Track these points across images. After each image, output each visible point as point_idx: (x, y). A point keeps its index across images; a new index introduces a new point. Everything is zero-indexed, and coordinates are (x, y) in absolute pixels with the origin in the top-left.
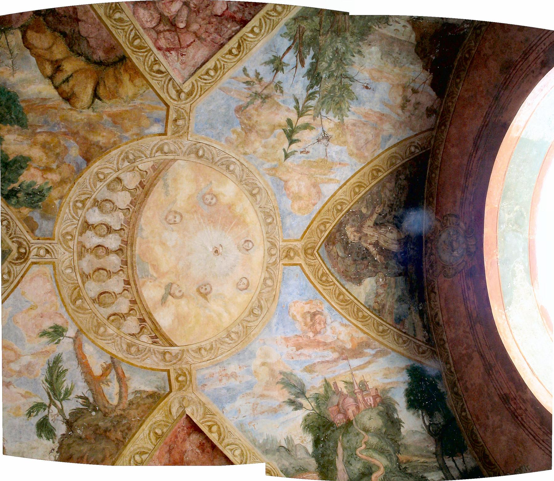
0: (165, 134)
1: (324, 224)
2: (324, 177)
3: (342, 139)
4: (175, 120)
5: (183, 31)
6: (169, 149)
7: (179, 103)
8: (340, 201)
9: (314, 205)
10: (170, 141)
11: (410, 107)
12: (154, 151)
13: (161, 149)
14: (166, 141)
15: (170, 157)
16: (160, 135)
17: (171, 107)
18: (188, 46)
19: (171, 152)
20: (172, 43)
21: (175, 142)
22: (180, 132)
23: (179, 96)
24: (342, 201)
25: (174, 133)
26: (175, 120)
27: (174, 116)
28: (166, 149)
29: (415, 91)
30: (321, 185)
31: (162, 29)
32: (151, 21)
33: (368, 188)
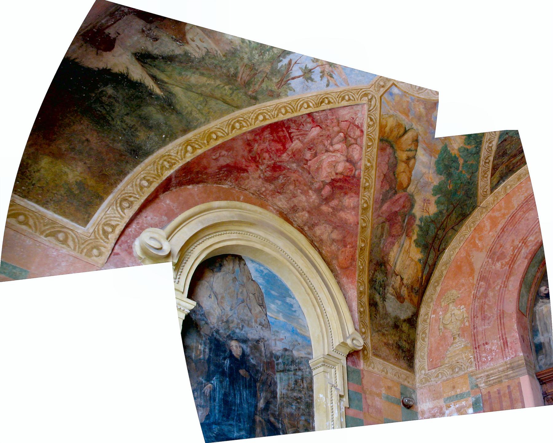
5: (343, 131)
18: (346, 121)
20: (353, 128)
31: (353, 140)
32: (355, 148)
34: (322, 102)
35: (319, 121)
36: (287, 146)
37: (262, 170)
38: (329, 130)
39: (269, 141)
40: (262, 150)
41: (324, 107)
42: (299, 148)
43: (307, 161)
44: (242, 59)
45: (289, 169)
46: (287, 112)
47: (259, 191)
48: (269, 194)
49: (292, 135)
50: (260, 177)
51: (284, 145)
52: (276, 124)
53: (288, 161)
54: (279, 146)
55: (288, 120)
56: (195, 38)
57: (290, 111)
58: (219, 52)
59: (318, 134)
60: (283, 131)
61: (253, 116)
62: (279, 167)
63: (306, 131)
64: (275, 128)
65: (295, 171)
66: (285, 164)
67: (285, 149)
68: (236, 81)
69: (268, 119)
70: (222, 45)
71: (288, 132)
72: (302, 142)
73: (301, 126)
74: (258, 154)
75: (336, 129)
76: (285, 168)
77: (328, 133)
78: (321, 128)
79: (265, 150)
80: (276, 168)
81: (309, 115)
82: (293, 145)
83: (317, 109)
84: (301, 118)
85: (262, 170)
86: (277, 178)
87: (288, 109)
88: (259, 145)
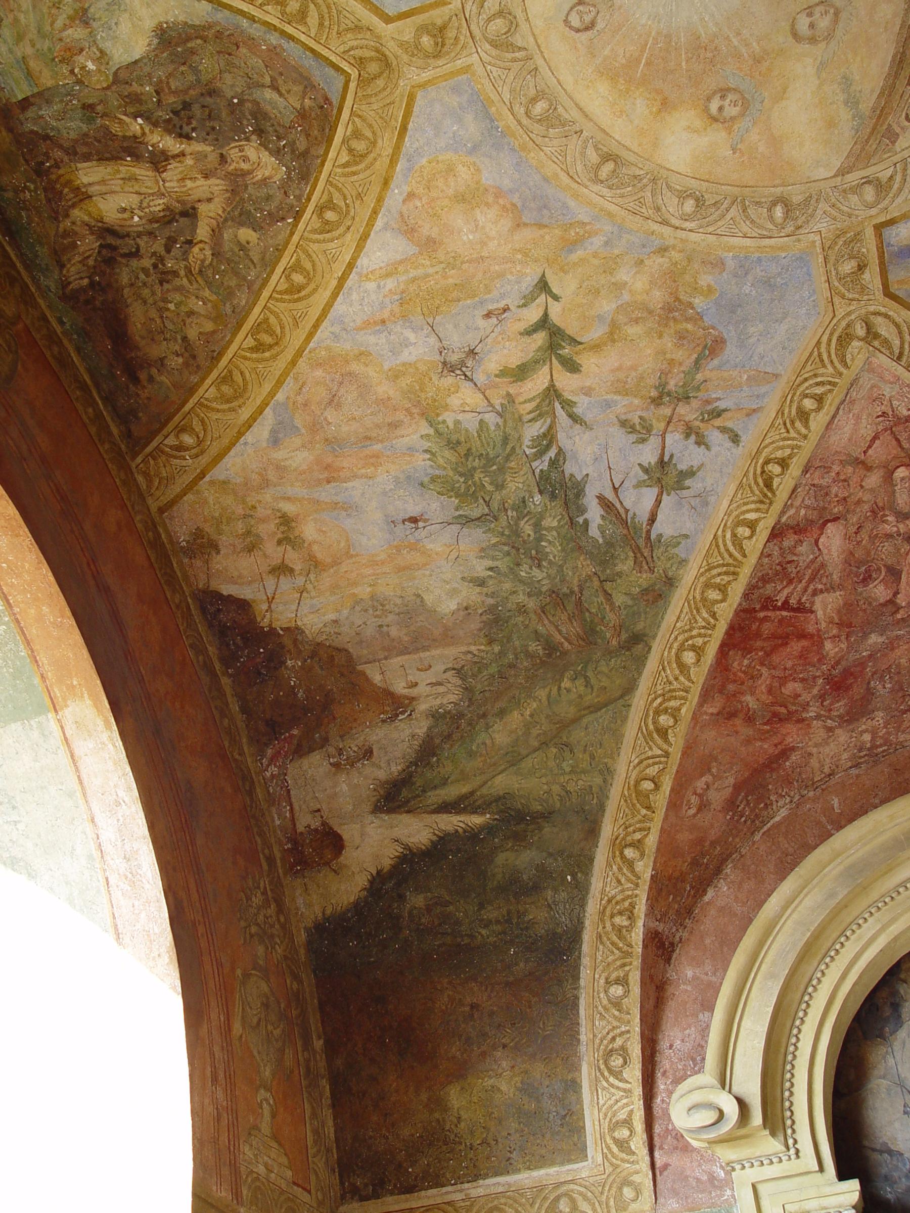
0: (879, 229)
1: (357, 157)
2: (413, 273)
3: (404, 382)
4: (861, 268)
6: (861, 195)
7: (863, 311)
8: (335, 234)
9: (411, 196)
10: (862, 214)
11: (267, 529)
12: (898, 178)
13: (882, 187)
14: (874, 211)
15: (853, 178)
16: (891, 222)
17: (879, 294)
19: (856, 189)
21: (850, 216)
22: (845, 242)
23: (869, 327)
24: (327, 236)
25: (858, 237)
26: (861, 268)
27: (867, 276)
28: (869, 193)
29: (282, 569)
30: (412, 250)
33: (266, 294)
34: (768, 485)
35: (814, 515)
36: (811, 629)
37: (818, 717)
38: (859, 502)
39: (762, 664)
40: (770, 691)
41: (783, 485)
42: (841, 602)
43: (891, 602)
44: (522, 609)
45: (870, 656)
46: (723, 589)
47: (860, 750)
48: (888, 733)
49: (793, 601)
50: (830, 730)
51: (802, 636)
52: (732, 629)
53: (850, 647)
54: (796, 646)
55: (746, 596)
56: (410, 678)
57: (726, 578)
58: (473, 648)
59: (847, 538)
60: (766, 619)
61: (672, 671)
62: (847, 673)
63: (812, 562)
64: (739, 636)
65: (891, 646)
66: (852, 657)
67: (817, 639)
68: (565, 653)
69: (705, 643)
70: (461, 633)
71: (776, 608)
72: (831, 589)
73: (791, 569)
74: (773, 704)
75: (874, 480)
76: (862, 664)
77: (866, 507)
78: (836, 519)
79: (776, 684)
80: (838, 684)
81: (776, 534)
82: (820, 614)
83: (777, 507)
84: (766, 560)
85: (818, 717)
86: (870, 693)
87: (718, 580)
88: (752, 694)
